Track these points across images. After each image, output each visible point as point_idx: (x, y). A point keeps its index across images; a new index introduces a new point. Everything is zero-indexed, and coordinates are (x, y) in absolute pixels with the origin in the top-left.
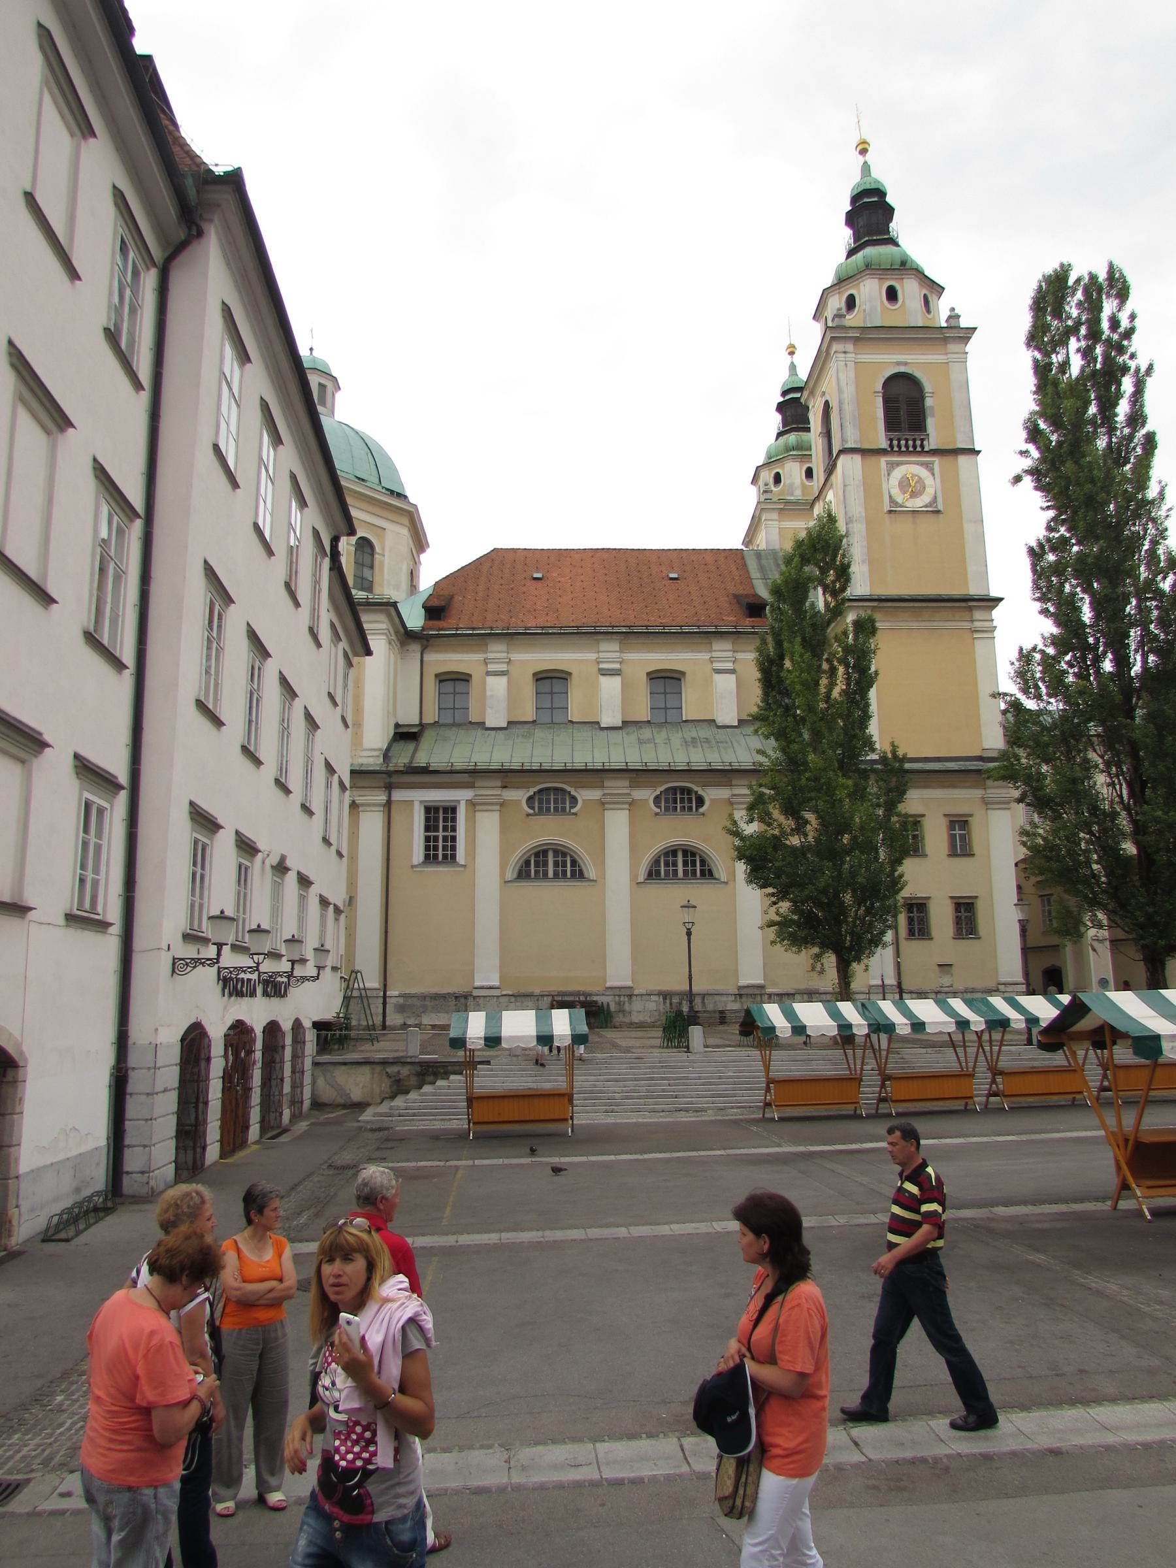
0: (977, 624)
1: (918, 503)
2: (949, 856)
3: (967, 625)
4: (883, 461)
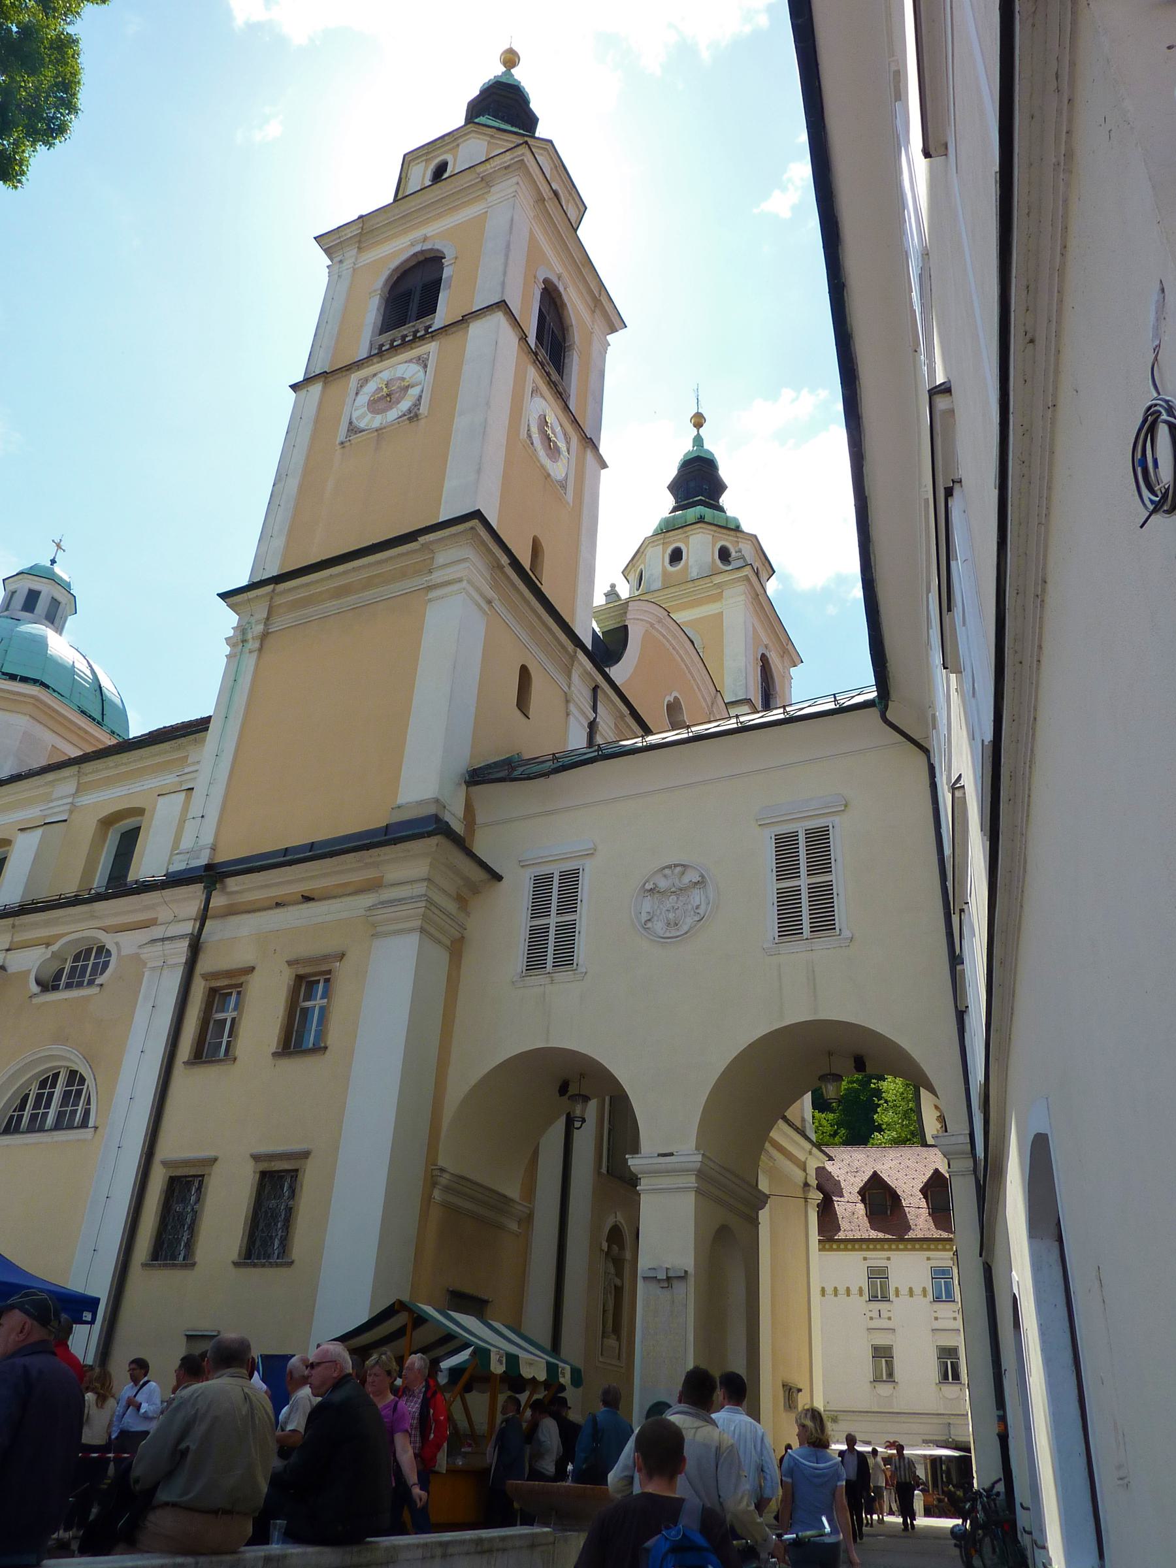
0: (437, 577)
1: (392, 415)
2: (275, 1054)
3: (424, 580)
4: (355, 377)
